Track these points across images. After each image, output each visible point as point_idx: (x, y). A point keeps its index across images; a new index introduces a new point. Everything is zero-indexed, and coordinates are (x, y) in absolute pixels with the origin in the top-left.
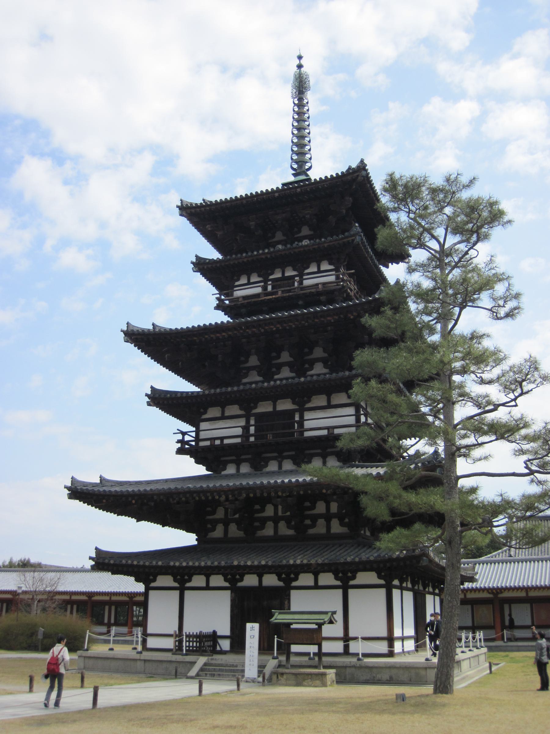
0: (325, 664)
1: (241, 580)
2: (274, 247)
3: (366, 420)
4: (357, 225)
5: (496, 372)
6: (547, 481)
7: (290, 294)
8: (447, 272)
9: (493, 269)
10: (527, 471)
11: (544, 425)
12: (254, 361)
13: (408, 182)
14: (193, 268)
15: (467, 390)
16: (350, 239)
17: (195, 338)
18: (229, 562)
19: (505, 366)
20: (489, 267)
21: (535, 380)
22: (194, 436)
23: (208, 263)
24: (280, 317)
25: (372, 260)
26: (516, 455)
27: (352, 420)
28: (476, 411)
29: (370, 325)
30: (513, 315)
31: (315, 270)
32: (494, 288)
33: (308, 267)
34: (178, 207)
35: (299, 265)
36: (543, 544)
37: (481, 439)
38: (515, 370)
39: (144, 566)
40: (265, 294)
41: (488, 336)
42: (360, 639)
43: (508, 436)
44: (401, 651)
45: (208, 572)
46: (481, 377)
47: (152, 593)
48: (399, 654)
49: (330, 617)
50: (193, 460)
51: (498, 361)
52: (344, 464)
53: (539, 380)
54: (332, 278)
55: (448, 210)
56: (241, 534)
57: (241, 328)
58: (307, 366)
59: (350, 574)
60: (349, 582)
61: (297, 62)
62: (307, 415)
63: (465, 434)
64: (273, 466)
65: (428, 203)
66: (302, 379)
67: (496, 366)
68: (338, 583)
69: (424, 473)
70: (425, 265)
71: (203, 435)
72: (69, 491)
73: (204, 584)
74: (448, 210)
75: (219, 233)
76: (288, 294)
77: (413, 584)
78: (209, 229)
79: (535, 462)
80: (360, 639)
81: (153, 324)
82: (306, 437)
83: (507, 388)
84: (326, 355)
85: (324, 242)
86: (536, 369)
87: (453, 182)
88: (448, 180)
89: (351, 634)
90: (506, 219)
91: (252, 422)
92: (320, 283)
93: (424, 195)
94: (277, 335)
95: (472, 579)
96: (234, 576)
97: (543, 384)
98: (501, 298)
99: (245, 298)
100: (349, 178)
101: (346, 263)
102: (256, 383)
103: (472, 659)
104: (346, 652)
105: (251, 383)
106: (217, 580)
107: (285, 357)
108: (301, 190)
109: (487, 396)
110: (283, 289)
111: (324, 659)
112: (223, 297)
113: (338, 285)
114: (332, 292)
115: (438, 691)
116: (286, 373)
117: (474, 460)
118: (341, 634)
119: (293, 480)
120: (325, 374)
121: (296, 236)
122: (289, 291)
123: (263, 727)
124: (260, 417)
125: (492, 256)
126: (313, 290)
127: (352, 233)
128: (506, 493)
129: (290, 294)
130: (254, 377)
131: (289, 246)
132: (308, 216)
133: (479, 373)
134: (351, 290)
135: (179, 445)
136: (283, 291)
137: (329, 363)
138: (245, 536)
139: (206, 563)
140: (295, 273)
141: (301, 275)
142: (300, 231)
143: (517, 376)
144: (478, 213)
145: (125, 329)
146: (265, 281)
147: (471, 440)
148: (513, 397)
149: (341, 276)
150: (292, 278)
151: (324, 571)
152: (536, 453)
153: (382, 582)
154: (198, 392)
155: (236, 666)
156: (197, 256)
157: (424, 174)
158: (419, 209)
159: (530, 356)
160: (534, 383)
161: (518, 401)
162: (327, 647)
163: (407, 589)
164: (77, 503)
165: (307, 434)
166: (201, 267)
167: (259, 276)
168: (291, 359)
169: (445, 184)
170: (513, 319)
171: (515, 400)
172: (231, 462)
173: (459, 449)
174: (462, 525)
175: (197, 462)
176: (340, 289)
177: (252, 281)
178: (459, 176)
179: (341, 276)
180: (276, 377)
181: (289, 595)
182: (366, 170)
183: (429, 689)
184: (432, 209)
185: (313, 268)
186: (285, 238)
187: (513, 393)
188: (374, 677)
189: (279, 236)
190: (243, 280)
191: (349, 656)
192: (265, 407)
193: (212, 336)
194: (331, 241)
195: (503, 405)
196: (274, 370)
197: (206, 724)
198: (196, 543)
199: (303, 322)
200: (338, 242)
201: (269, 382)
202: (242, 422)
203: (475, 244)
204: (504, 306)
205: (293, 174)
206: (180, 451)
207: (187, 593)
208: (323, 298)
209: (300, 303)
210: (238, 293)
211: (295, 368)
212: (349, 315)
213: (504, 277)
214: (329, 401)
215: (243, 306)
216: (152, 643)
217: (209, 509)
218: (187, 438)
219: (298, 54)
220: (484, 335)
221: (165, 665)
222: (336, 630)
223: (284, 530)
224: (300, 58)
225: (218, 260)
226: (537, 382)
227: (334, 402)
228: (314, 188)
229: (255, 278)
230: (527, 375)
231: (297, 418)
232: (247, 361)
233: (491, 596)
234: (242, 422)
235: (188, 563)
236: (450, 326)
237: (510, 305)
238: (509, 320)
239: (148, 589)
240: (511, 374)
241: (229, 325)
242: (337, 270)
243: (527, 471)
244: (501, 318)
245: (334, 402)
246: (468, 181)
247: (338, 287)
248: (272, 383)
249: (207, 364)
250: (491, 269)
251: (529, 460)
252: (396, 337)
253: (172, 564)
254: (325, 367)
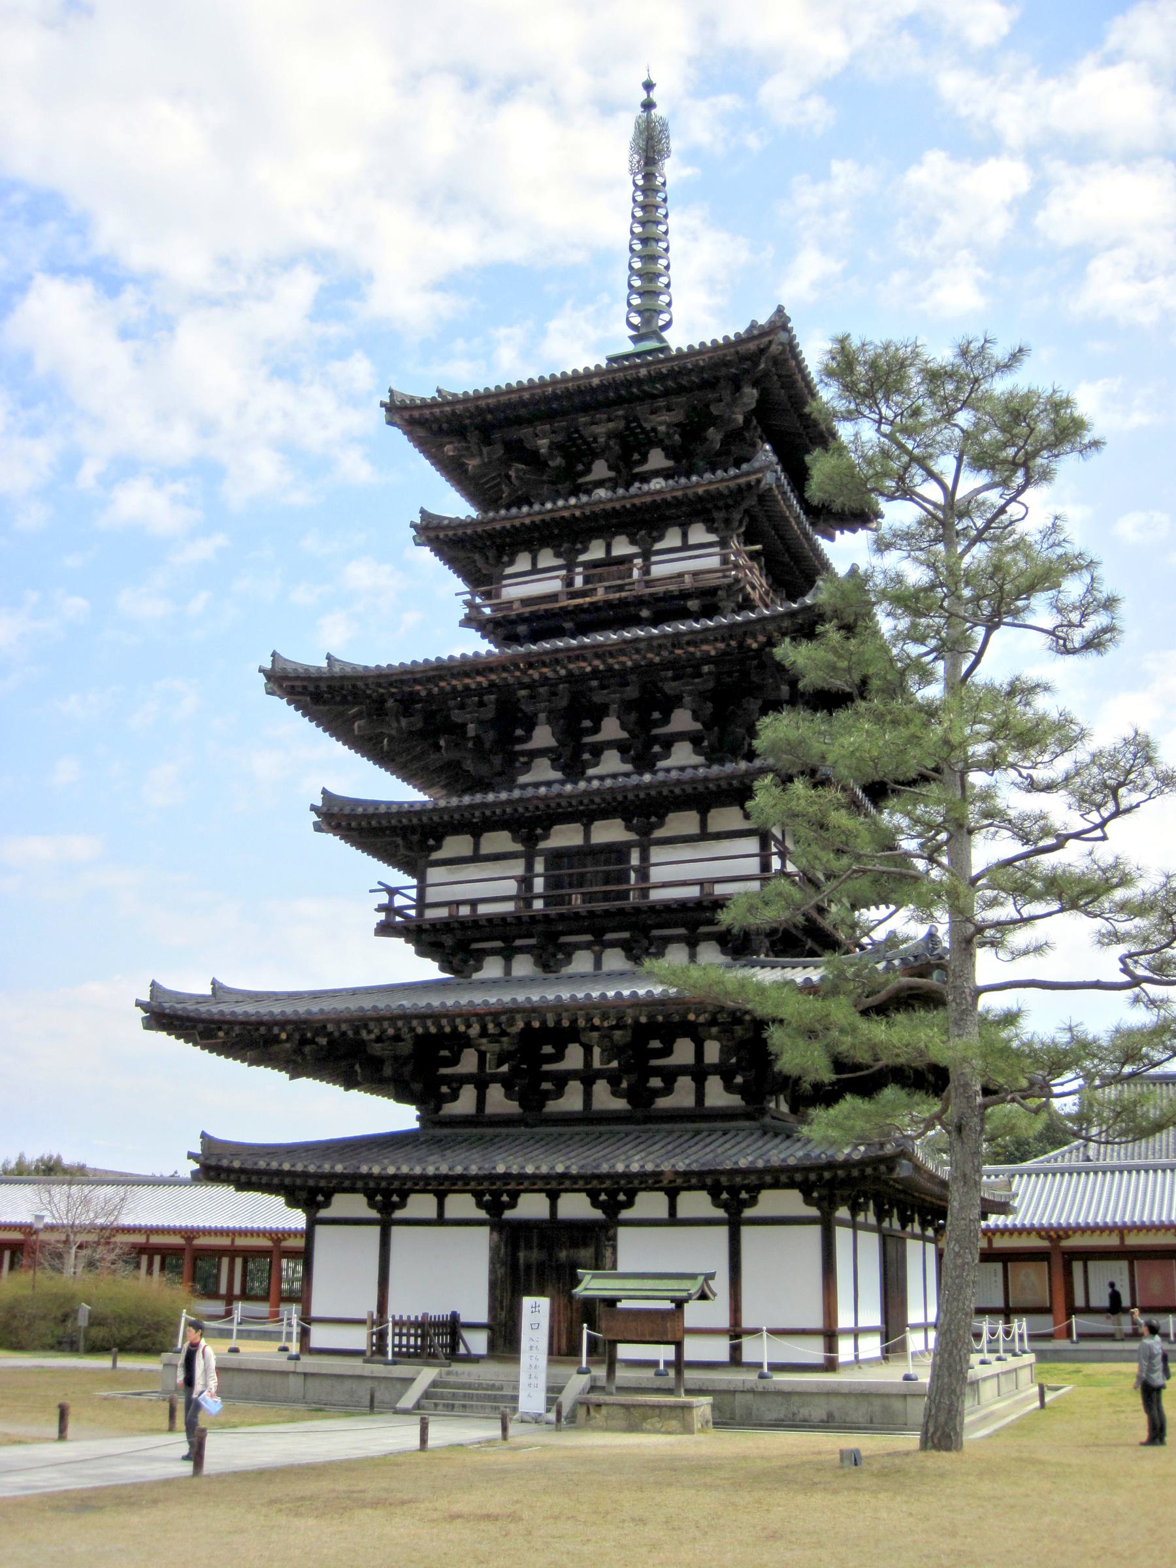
0: (690, 1386)
1: (513, 1205)
2: (588, 492)
3: (783, 865)
4: (767, 447)
5: (1064, 764)
6: (1168, 1000)
7: (624, 594)
8: (959, 550)
9: (1059, 545)
10: (1125, 978)
11: (1164, 879)
12: (543, 736)
13: (878, 356)
14: (414, 538)
15: (1000, 803)
16: (753, 478)
17: (418, 688)
18: (487, 1166)
19: (1081, 753)
20: (1051, 541)
21: (1146, 785)
22: (415, 896)
23: (448, 527)
24: (600, 646)
25: (799, 523)
26: (1103, 944)
27: (752, 866)
28: (1018, 848)
29: (794, 662)
30: (1100, 644)
31: (678, 543)
32: (1060, 586)
33: (661, 538)
34: (383, 405)
35: (643, 532)
36: (1158, 1135)
37: (1029, 910)
38: (1103, 761)
39: (305, 1175)
40: (568, 593)
41: (1047, 689)
42: (765, 1334)
43: (1087, 904)
44: (852, 1358)
45: (441, 1187)
46: (1029, 776)
47: (320, 1230)
48: (848, 1364)
49: (702, 1286)
50: (411, 948)
51: (1067, 743)
52: (734, 960)
53: (1155, 784)
54: (714, 562)
55: (964, 418)
56: (512, 1107)
57: (517, 667)
58: (657, 749)
59: (744, 1195)
60: (741, 1212)
61: (643, 95)
62: (657, 854)
63: (995, 898)
64: (582, 962)
65: (920, 402)
66: (647, 778)
67: (1062, 753)
68: (720, 1213)
69: (905, 980)
70: (913, 536)
71: (432, 895)
72: (146, 1012)
73: (432, 1214)
74: (964, 418)
75: (472, 463)
76: (617, 595)
77: (881, 1215)
78: (451, 453)
79: (1143, 959)
80: (765, 1334)
81: (329, 657)
82: (653, 901)
83: (1084, 801)
84: (698, 726)
85: (698, 484)
86: (1149, 760)
87: (974, 357)
88: (964, 353)
89: (747, 1322)
90: (1087, 438)
91: (539, 867)
92: (688, 573)
93: (913, 384)
94: (595, 683)
95: (1003, 1208)
96: (496, 1195)
97: (1162, 792)
98: (1075, 608)
99: (526, 602)
100: (752, 346)
101: (743, 529)
102: (549, 784)
103: (1002, 1378)
104: (736, 1358)
105: (537, 785)
106: (461, 1205)
107: (611, 728)
108: (649, 372)
109: (1043, 817)
110: (607, 584)
111: (688, 1374)
112: (478, 600)
113: (725, 577)
114: (712, 591)
115: (930, 1444)
116: (612, 762)
117: (1012, 953)
118: (724, 1322)
119: (626, 993)
120: (695, 767)
121: (637, 470)
122: (621, 588)
123: (556, 1518)
124: (557, 858)
125: (1056, 518)
126: (671, 587)
127: (756, 464)
128: (1081, 1024)
129: (624, 594)
130: (543, 771)
131: (621, 491)
132: (662, 428)
133: (1025, 768)
134: (754, 587)
135: (382, 916)
136: (607, 588)
137: (706, 743)
138: (521, 1111)
139: (437, 1169)
140: (634, 550)
141: (646, 555)
142: (644, 460)
143: (1107, 774)
144: (1028, 425)
145: (268, 666)
146: (570, 566)
147: (1006, 911)
148: (1098, 820)
149: (733, 558)
150: (626, 560)
151: (690, 1188)
152: (1146, 940)
153: (814, 1212)
154: (424, 803)
155: (501, 1388)
156: (423, 511)
157: (913, 340)
158: (902, 414)
159: (1136, 733)
160: (1142, 789)
161: (1109, 828)
162: (694, 1349)
163: (867, 1228)
164: (162, 1038)
165: (656, 895)
166: (432, 534)
167: (557, 555)
168: (624, 735)
169: (958, 361)
170: (1099, 652)
171: (1102, 825)
172: (494, 952)
173: (980, 930)
174: (986, 1091)
175: (421, 953)
176: (729, 586)
177: (540, 565)
178: (988, 345)
179: (733, 558)
180: (591, 772)
181: (614, 1238)
182: (789, 331)
183: (912, 1440)
184: (929, 415)
185: (672, 539)
186: (612, 474)
187: (1098, 810)
188: (794, 1414)
189: (600, 469)
190: (523, 563)
191: (741, 1369)
192: (566, 837)
193: (454, 682)
194: (711, 483)
195: (1077, 836)
196: (586, 756)
197: (436, 1510)
198: (416, 1125)
199: (650, 655)
200: (725, 484)
201: (576, 783)
202: (517, 868)
203: (1021, 490)
204: (1081, 625)
205: (632, 338)
206: (385, 929)
207: (396, 1232)
208: (693, 605)
209: (645, 613)
210: (513, 592)
211: (632, 753)
212: (749, 641)
213: (1082, 562)
214: (703, 823)
215: (522, 619)
216: (320, 1337)
217: (445, 1053)
218: (399, 901)
219: (645, 78)
220: (1038, 686)
221: (348, 1384)
222: (715, 1313)
223: (605, 1099)
225: (469, 520)
226: (1149, 789)
227: (714, 826)
228: (676, 369)
229: (547, 558)
230: (1129, 772)
231: (635, 859)
232: (528, 738)
233: (1045, 1244)
234: (517, 868)
235: (398, 1169)
236: (965, 667)
237: (1097, 621)
238: (1091, 657)
239: (313, 1222)
240: (1095, 770)
241: (491, 659)
242: (723, 543)
243: (1125, 978)
244: (1074, 651)
245: (714, 826)
246: (1007, 357)
247: (726, 581)
248: (582, 785)
249: (442, 743)
250: (1053, 545)
251: (1130, 956)
252: (848, 690)
253: (364, 1169)
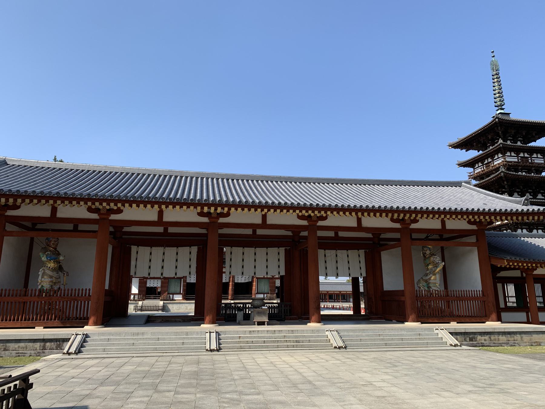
140: (529, 156)
141: (531, 158)
146: (518, 156)
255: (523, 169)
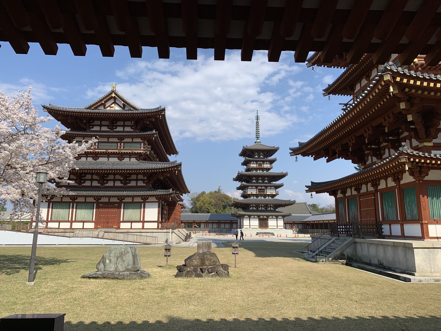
106: (256, 217)
124: (259, 189)
150: (262, 164)
185: (266, 163)
190: (252, 162)
224: (257, 111)
254: (268, 181)
255: (260, 169)
